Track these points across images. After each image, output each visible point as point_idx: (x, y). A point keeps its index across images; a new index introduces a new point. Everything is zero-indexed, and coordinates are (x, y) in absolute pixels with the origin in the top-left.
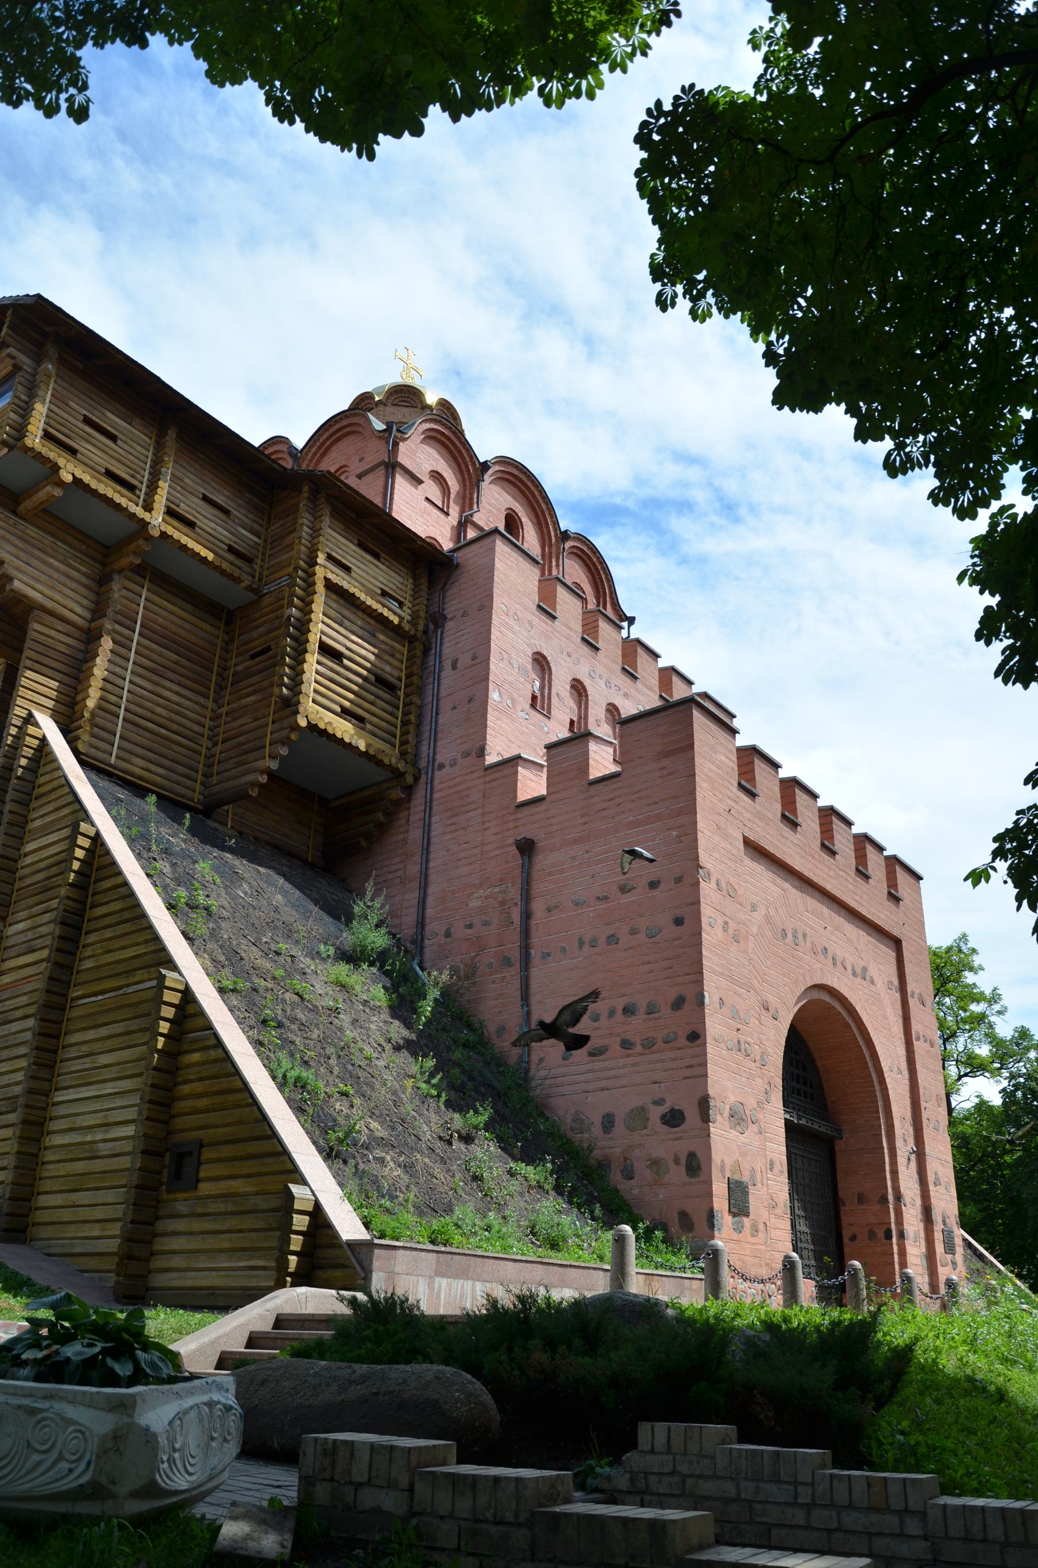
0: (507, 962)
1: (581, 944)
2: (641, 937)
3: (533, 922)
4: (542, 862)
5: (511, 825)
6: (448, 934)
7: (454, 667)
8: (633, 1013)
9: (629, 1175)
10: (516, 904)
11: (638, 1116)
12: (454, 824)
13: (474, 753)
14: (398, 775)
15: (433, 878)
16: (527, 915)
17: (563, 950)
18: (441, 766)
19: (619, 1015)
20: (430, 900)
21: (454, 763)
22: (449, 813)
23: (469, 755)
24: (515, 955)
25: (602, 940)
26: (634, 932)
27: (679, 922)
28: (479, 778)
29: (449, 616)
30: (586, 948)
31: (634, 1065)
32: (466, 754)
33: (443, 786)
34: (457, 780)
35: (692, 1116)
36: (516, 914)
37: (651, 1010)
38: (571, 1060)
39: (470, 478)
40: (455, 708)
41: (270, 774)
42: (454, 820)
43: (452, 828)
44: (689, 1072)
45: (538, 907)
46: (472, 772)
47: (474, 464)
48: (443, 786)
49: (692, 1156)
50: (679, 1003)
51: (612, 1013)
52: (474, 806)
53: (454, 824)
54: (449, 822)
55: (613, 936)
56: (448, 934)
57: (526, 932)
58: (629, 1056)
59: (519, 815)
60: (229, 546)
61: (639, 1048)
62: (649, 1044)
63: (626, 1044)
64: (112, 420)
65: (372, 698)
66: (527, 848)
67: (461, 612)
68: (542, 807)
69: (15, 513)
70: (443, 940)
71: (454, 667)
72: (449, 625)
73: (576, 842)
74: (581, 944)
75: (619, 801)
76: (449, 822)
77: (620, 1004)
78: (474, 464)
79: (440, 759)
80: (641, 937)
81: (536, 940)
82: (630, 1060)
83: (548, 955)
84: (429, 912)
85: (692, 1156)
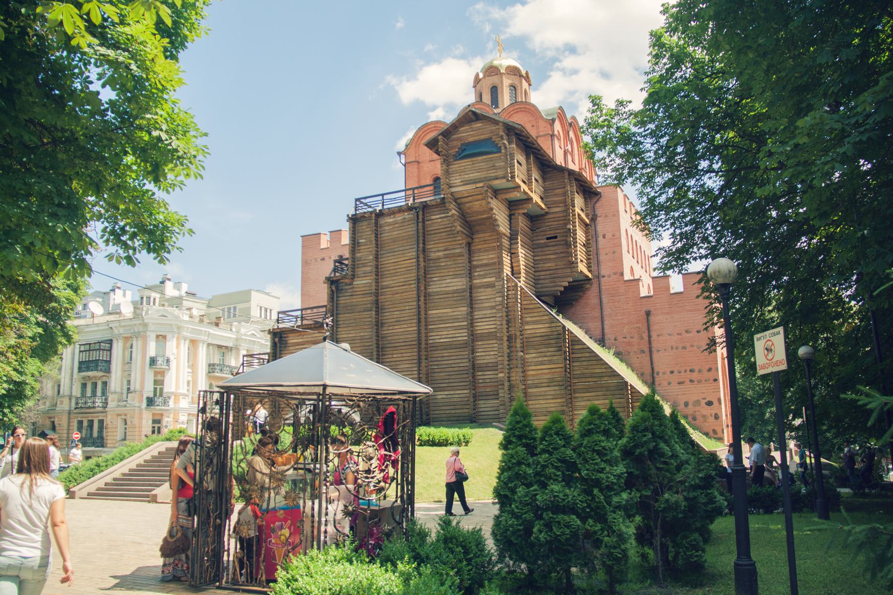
4: (652, 318)
6: (615, 340)
7: (604, 237)
11: (697, 403)
15: (605, 318)
16: (650, 337)
18: (603, 277)
21: (609, 276)
24: (646, 349)
26: (692, 346)
35: (716, 403)
36: (645, 336)
37: (700, 371)
41: (565, 287)
45: (654, 335)
49: (716, 414)
50: (710, 370)
57: (650, 342)
62: (699, 382)
63: (691, 381)
66: (648, 314)
71: (604, 237)
72: (599, 219)
73: (667, 313)
74: (672, 348)
79: (603, 273)
80: (695, 348)
81: (654, 345)
84: (606, 331)
85: (716, 414)
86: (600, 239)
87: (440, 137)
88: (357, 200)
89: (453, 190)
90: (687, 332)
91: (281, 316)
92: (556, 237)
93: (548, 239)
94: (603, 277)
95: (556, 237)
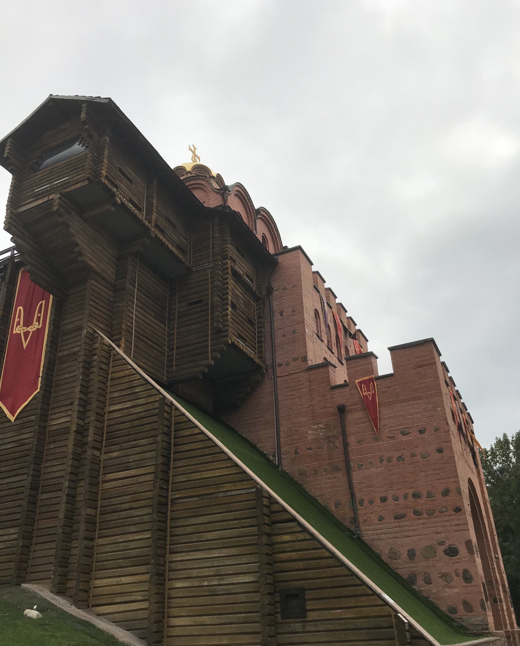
0: (337, 469)
1: (382, 461)
2: (418, 457)
3: (350, 448)
5: (329, 397)
6: (296, 453)
7: (281, 314)
8: (419, 497)
9: (428, 582)
10: (338, 438)
11: (430, 551)
12: (292, 395)
13: (300, 360)
14: (259, 368)
15: (282, 422)
17: (371, 463)
19: (410, 498)
20: (282, 434)
23: (297, 360)
25: (395, 460)
27: (440, 451)
29: (274, 289)
30: (385, 463)
31: (423, 524)
32: (295, 360)
37: (429, 495)
38: (384, 521)
39: (251, 217)
40: (285, 336)
43: (292, 397)
44: (457, 528)
45: (352, 440)
47: (253, 210)
49: (466, 571)
51: (406, 496)
52: (304, 386)
53: (292, 395)
55: (400, 457)
56: (296, 453)
58: (419, 519)
59: (333, 392)
60: (177, 245)
61: (425, 515)
63: (417, 513)
64: (130, 172)
65: (247, 329)
67: (282, 287)
68: (347, 389)
69: (81, 217)
70: (294, 456)
72: (275, 293)
74: (382, 461)
75: (394, 388)
77: (411, 492)
78: (253, 210)
79: (278, 361)
81: (352, 457)
82: (420, 521)
83: (362, 465)
85: (466, 571)
86: (277, 317)
90: (404, 434)
94: (280, 365)
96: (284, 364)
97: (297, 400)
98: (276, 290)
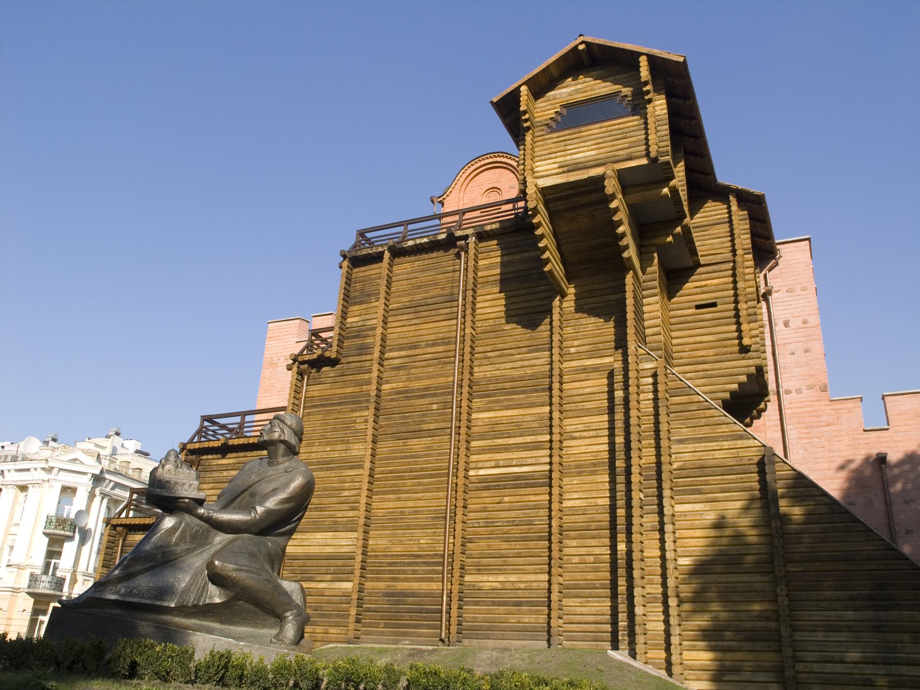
7: (786, 324)
18: (788, 392)
21: (799, 391)
22: (801, 425)
28: (826, 405)
33: (792, 405)
34: (805, 404)
42: (808, 430)
43: (807, 435)
46: (818, 401)
48: (792, 405)
54: (803, 431)
67: (786, 288)
71: (786, 324)
76: (803, 431)
79: (785, 385)
86: (779, 328)
87: (524, 89)
88: (362, 234)
89: (543, 183)
91: (206, 424)
92: (714, 305)
93: (698, 307)
94: (788, 392)
95: (714, 305)
96: (794, 391)
97: (816, 440)
98: (777, 291)
